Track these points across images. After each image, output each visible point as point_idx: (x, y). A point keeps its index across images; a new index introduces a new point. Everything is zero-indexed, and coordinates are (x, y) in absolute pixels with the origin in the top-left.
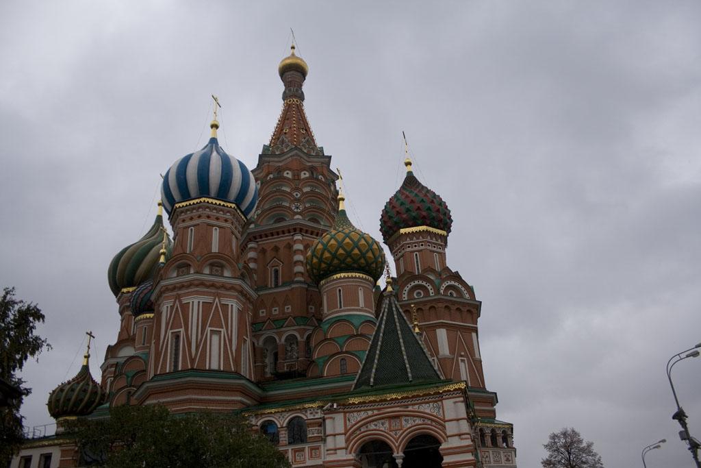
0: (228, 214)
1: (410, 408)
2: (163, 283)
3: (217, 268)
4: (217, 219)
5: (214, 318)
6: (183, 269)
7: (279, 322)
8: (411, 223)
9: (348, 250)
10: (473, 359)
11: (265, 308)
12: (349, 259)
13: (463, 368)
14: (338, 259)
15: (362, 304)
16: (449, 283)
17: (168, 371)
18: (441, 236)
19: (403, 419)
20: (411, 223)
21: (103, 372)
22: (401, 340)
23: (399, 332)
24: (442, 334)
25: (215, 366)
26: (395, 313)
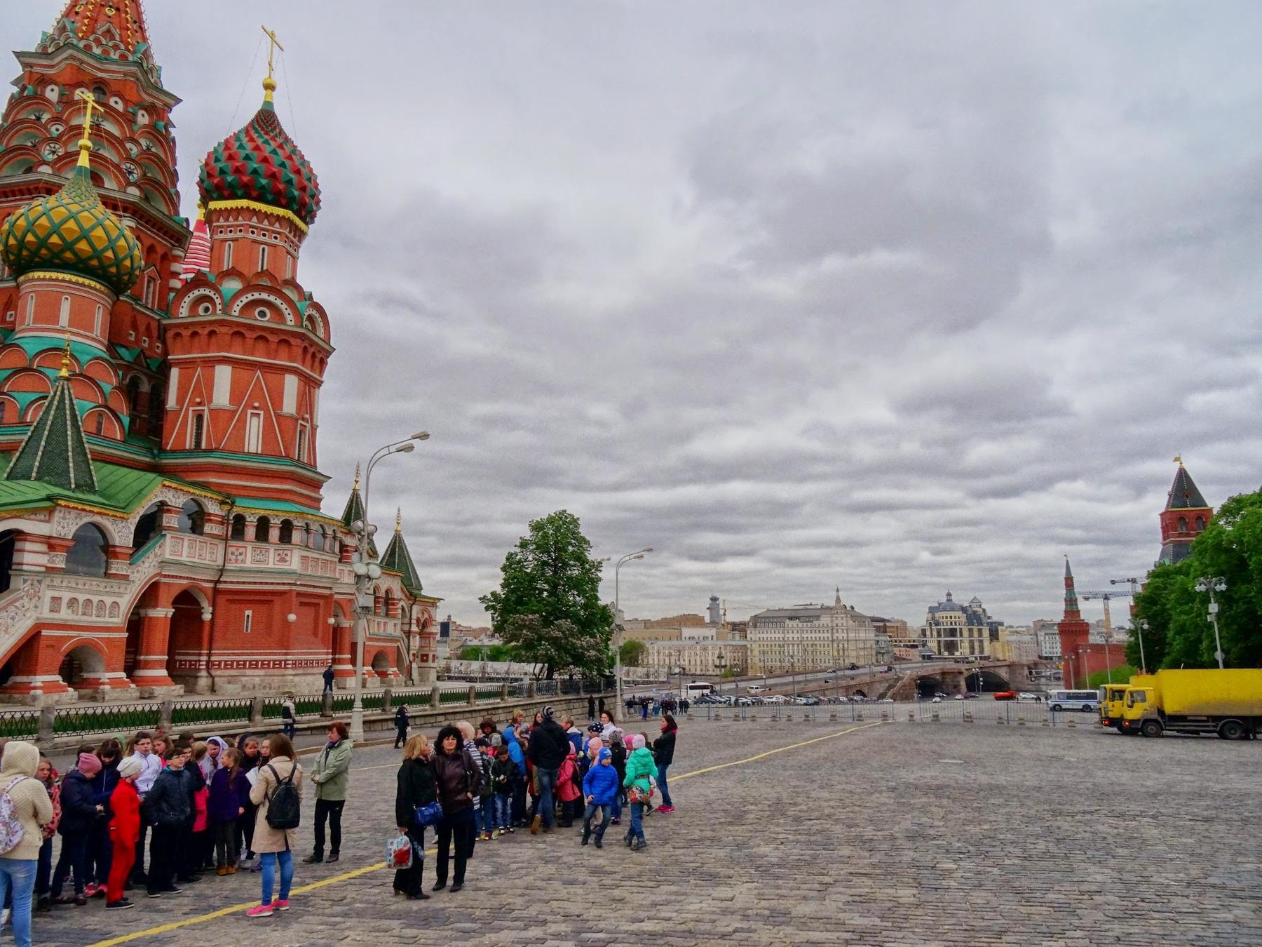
12: (44, 251)
16: (257, 296)
20: (226, 193)
24: (223, 375)
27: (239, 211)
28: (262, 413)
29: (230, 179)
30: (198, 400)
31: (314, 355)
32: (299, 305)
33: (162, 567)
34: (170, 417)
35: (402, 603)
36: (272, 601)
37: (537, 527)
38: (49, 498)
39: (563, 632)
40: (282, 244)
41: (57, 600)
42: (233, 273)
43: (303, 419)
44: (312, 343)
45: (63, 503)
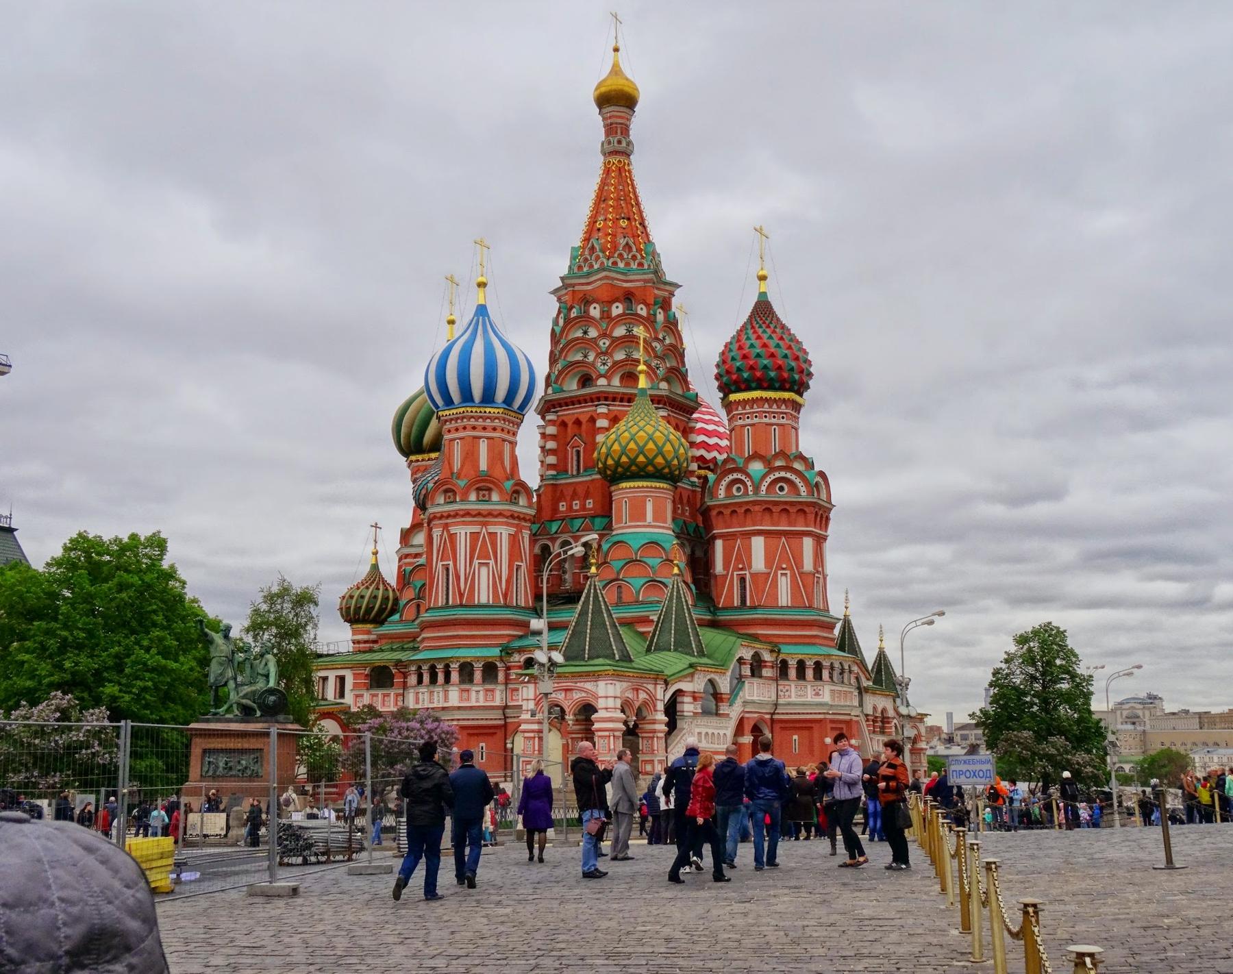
0: (497, 421)
1: (578, 684)
3: (484, 492)
4: (484, 428)
5: (482, 549)
6: (450, 494)
9: (632, 456)
11: (565, 501)
12: (634, 468)
14: (622, 467)
16: (777, 475)
18: (784, 401)
20: (743, 387)
21: (400, 559)
22: (589, 623)
23: (590, 615)
24: (758, 543)
25: (484, 600)
26: (592, 595)
27: (754, 401)
29: (746, 375)
30: (740, 566)
31: (822, 517)
32: (806, 474)
33: (744, 706)
34: (719, 581)
35: (895, 721)
36: (812, 728)
37: (1022, 640)
38: (691, 666)
39: (1058, 750)
40: (789, 422)
42: (756, 456)
43: (818, 572)
44: (820, 506)
45: (699, 668)
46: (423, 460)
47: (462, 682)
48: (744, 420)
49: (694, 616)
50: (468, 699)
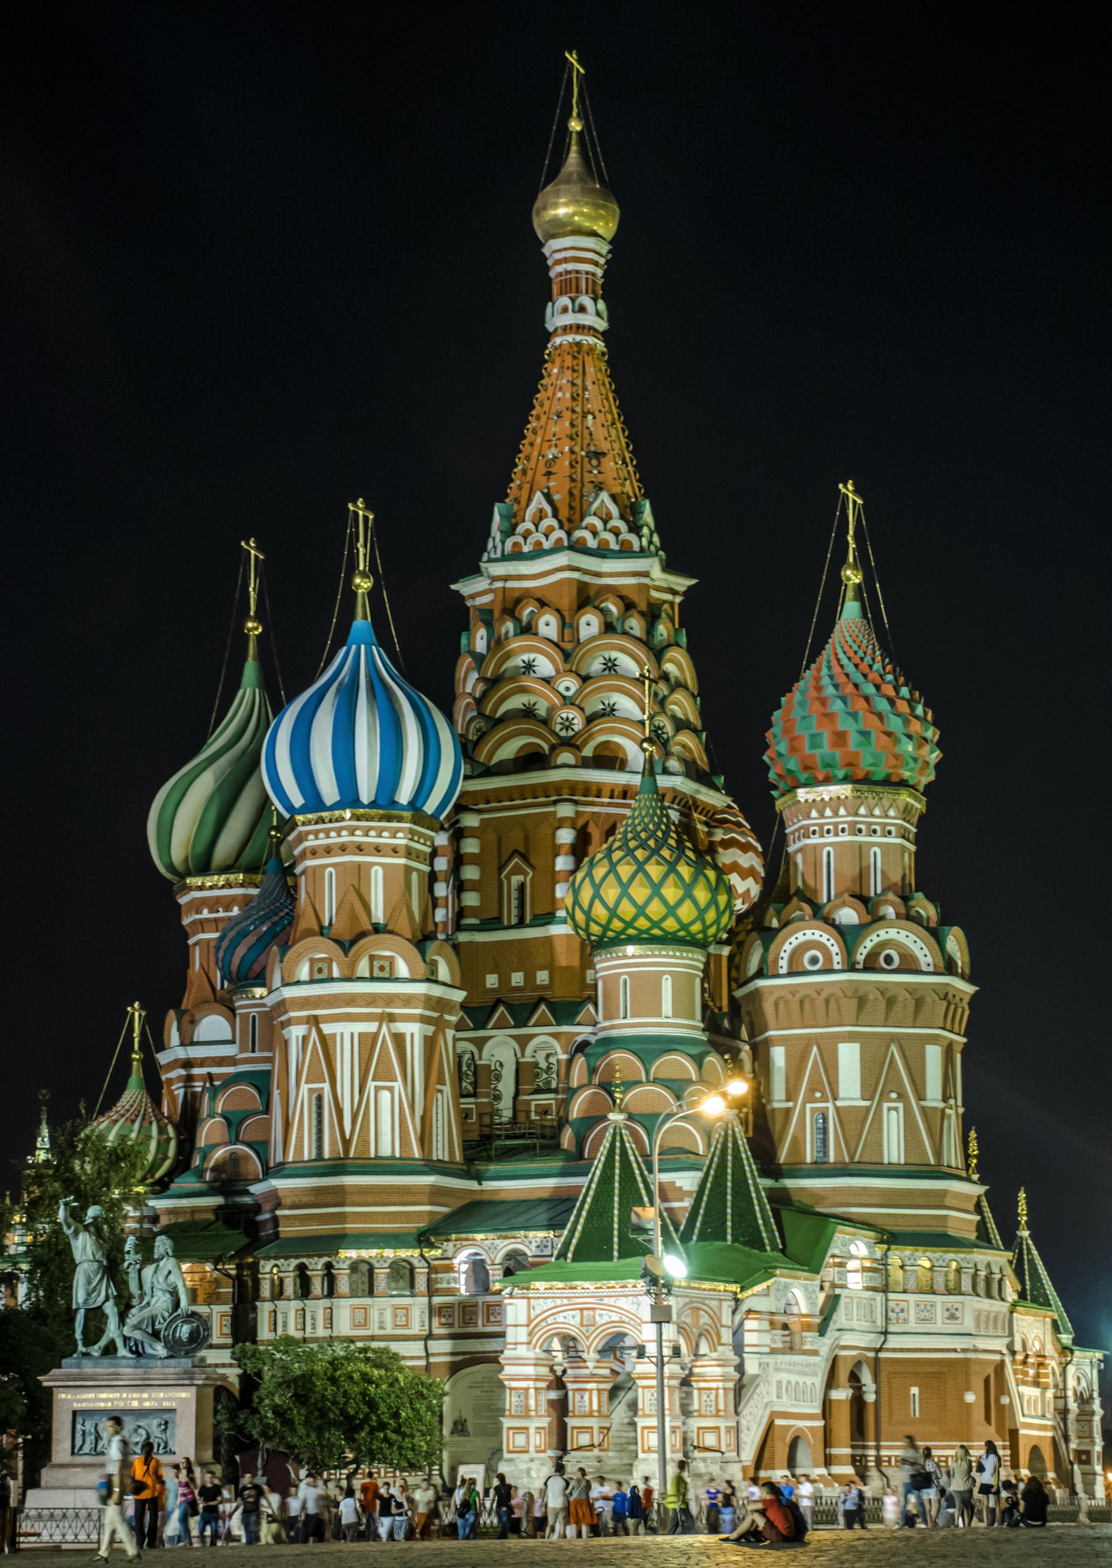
0: (400, 835)
1: (606, 1300)
2: (289, 993)
3: (382, 963)
4: (378, 850)
6: (320, 965)
7: (522, 1013)
8: (821, 778)
10: (918, 1105)
13: (893, 1124)
15: (667, 1006)
17: (306, 1158)
19: (598, 1312)
22: (616, 1199)
25: (386, 1150)
26: (618, 1151)
28: (900, 1105)
30: (818, 1095)
41: (779, 1382)
46: (211, 888)
47: (354, 1294)
48: (822, 836)
49: (758, 1180)
50: (365, 1324)
